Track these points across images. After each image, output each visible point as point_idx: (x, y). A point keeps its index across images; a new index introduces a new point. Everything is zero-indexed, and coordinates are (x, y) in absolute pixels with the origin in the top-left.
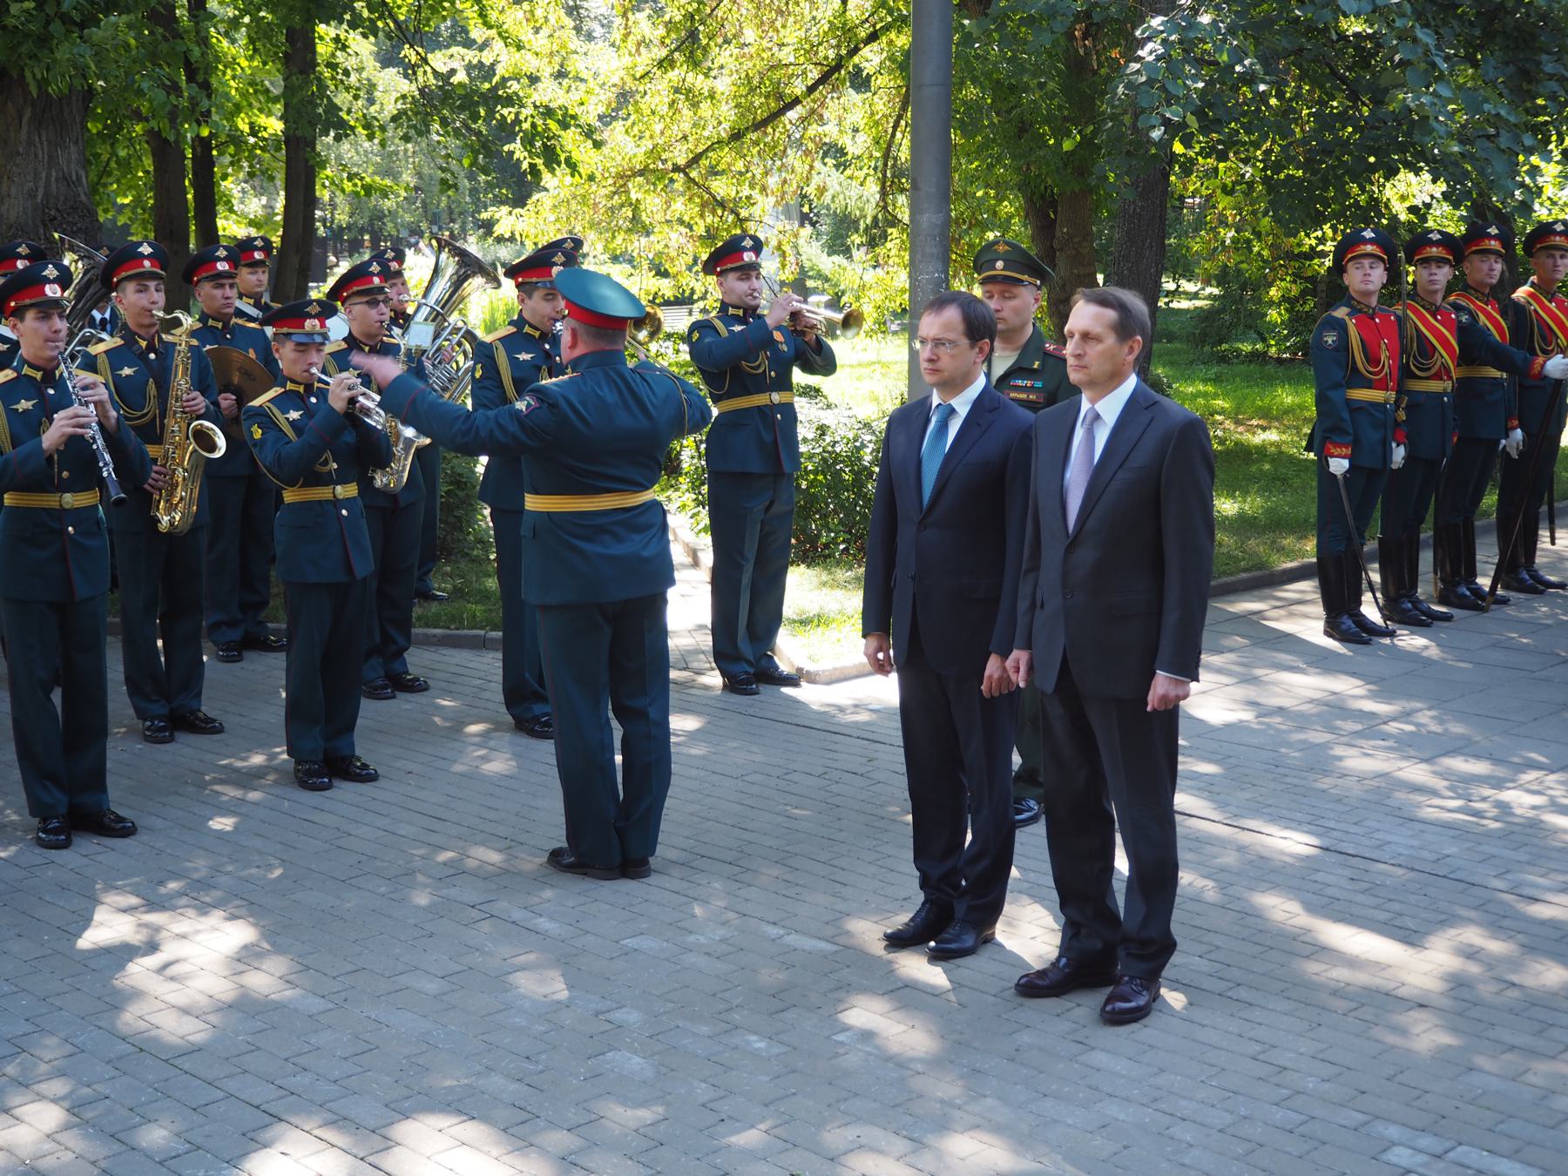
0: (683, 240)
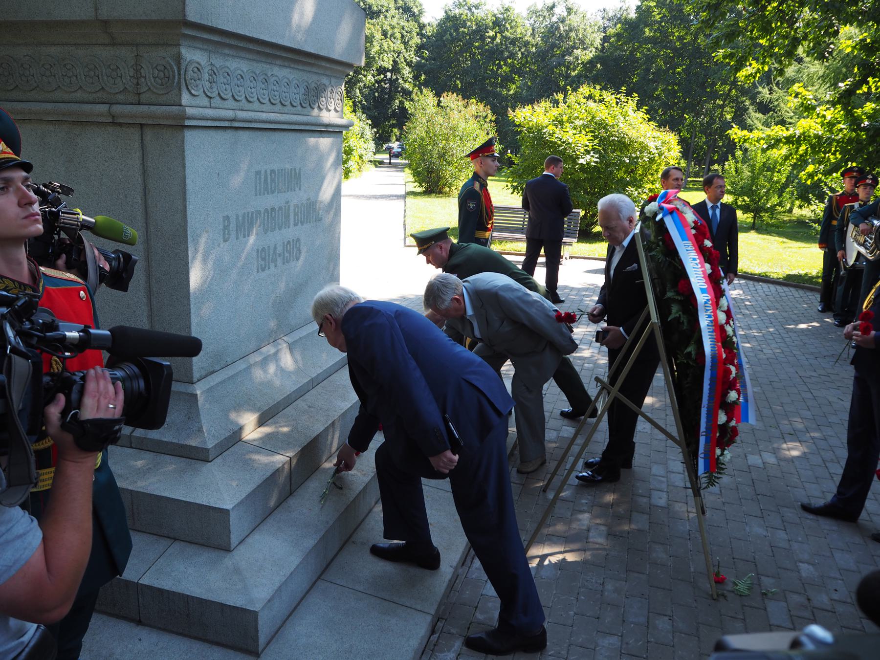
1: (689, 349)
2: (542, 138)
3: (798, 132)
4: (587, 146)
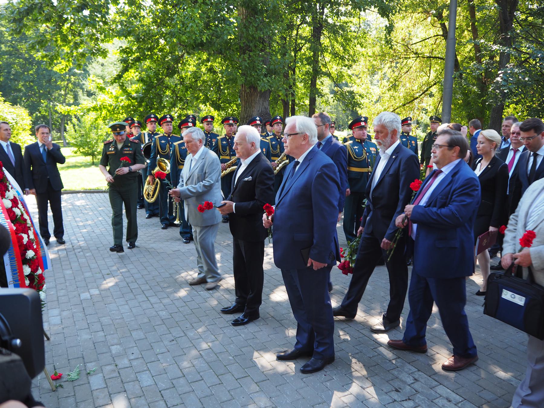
3: (99, 103)
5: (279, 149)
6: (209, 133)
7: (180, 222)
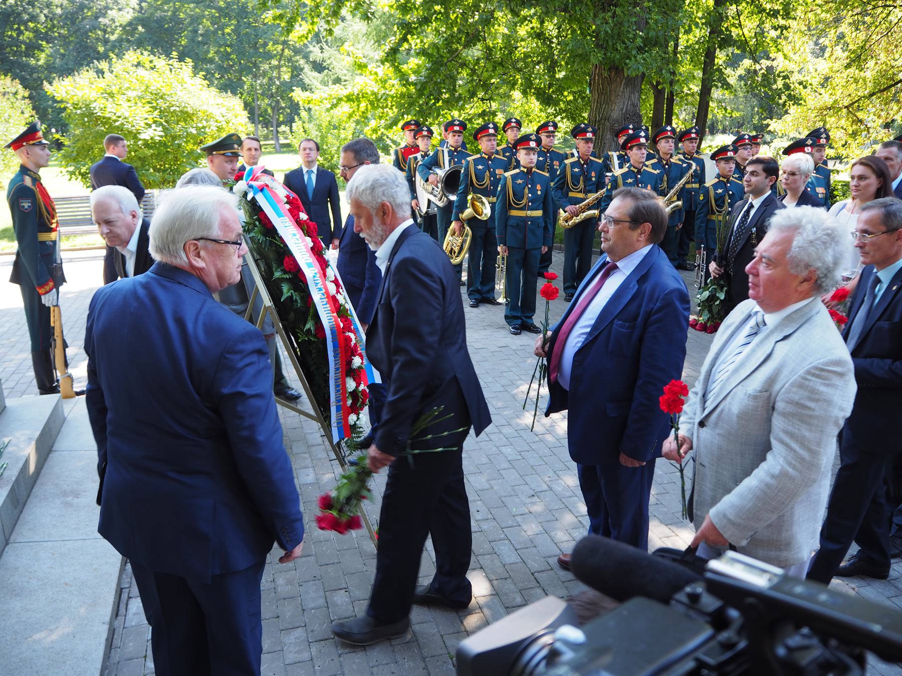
0: (842, 135)
1: (308, 326)
2: (93, 113)
4: (146, 119)
5: (665, 183)
6: (548, 150)
7: (507, 300)
